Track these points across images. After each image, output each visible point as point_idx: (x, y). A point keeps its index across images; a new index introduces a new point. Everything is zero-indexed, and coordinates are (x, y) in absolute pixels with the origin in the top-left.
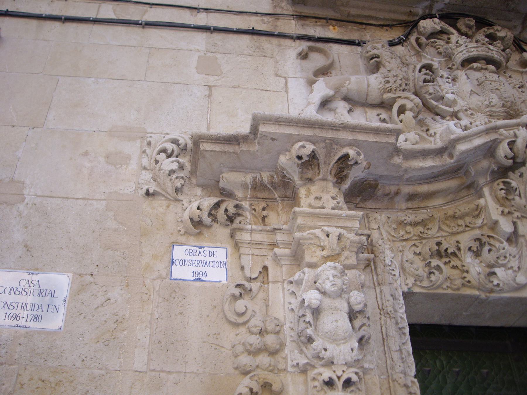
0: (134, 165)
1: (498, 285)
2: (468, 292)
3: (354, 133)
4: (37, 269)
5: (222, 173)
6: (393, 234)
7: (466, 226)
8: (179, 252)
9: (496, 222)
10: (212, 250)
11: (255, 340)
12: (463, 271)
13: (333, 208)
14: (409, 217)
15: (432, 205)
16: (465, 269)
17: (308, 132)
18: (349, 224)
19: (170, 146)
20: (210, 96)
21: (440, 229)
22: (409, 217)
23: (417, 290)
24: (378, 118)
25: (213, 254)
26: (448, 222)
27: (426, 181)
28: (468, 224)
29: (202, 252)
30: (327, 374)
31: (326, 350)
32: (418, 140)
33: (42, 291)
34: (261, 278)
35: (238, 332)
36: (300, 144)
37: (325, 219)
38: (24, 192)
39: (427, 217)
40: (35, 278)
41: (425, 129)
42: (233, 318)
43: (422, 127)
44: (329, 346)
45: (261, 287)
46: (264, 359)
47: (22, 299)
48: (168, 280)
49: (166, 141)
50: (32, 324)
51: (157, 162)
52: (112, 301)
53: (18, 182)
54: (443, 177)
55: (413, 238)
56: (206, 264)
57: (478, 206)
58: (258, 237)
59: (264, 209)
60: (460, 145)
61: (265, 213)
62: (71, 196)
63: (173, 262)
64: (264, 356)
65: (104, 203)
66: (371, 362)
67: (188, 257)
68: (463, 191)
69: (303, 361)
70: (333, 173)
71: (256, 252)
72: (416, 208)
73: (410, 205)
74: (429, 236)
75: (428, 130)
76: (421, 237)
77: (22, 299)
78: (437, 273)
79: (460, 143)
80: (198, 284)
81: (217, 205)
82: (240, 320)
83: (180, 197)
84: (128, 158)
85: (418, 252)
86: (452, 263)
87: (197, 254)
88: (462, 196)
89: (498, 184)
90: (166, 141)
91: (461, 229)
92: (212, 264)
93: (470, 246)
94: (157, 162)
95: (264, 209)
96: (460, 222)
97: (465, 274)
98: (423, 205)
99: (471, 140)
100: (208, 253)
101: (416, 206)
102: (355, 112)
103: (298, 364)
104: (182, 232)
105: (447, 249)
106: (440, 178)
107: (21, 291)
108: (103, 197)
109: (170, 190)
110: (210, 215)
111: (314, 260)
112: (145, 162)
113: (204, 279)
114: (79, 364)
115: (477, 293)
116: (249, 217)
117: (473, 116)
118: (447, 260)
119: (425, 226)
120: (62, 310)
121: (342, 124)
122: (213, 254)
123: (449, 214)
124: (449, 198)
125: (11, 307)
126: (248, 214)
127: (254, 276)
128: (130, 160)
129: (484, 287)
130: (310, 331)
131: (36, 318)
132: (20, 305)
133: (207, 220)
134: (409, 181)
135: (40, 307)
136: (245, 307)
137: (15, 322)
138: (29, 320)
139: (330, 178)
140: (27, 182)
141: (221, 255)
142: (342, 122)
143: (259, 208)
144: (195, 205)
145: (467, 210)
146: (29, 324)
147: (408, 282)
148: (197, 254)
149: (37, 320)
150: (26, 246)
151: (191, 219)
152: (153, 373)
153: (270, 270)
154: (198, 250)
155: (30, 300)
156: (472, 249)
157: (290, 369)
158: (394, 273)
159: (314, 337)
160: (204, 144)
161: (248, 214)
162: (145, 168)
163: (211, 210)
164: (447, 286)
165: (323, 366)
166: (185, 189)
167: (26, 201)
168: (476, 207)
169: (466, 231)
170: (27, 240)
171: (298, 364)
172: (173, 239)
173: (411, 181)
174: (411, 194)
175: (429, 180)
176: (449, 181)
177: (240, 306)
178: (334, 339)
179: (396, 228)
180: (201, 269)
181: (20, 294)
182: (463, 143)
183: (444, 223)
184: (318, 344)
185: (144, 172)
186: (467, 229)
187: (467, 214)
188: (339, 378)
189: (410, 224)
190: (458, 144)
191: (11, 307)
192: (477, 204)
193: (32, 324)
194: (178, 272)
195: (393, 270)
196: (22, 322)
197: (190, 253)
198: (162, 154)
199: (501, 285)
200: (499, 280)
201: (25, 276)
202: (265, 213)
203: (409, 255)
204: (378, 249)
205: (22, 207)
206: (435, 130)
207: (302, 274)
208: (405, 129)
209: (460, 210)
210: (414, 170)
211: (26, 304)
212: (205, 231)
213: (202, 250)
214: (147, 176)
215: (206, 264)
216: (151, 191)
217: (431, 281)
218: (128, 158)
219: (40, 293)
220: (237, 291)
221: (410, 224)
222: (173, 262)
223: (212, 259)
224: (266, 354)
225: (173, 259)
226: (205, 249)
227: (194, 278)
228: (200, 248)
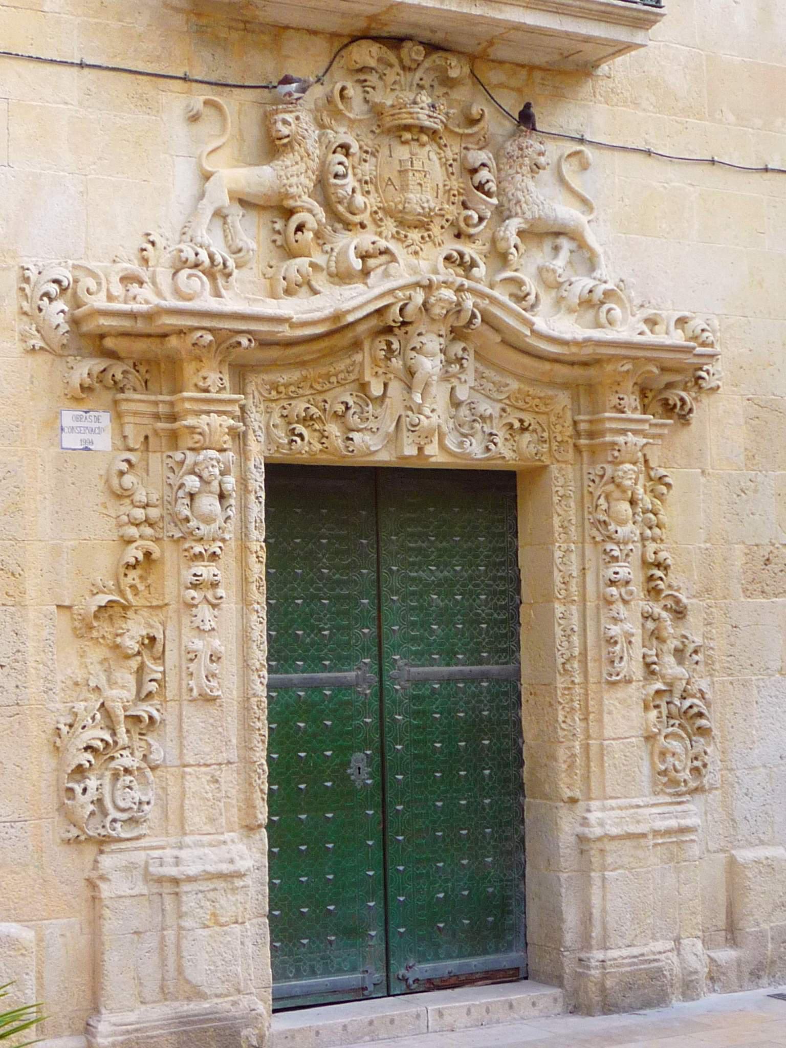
10: (97, 414)
25: (98, 419)
56: (92, 431)
63: (62, 429)
71: (138, 420)
113: (91, 447)
122: (98, 419)
141: (106, 418)
180: (87, 436)
197: (78, 418)
202: (147, 376)
213: (88, 415)
215: (92, 431)
223: (97, 425)
226: (91, 413)
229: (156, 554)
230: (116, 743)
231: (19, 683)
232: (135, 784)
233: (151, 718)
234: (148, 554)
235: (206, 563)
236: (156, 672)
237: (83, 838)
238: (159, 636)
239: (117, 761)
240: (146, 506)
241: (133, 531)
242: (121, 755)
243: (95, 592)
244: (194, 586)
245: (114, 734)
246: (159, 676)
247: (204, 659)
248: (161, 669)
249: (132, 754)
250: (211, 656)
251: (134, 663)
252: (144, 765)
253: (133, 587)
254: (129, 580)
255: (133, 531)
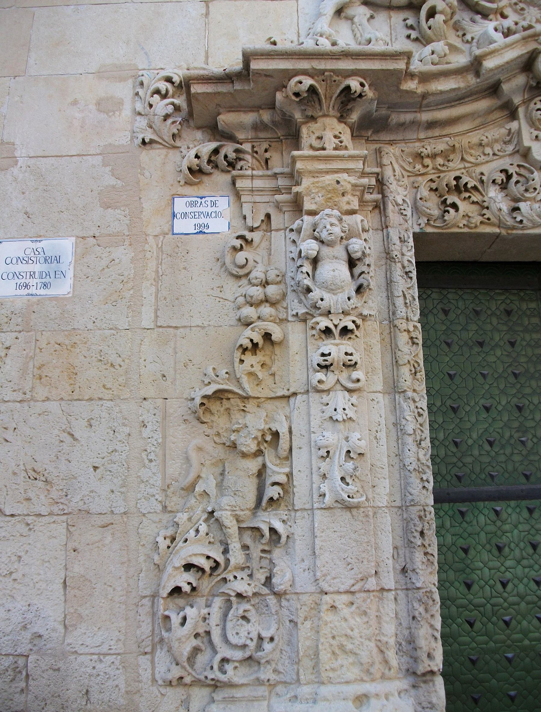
0: (127, 112)
1: (521, 221)
2: (488, 229)
3: (357, 61)
4: (40, 236)
5: (219, 114)
6: (408, 169)
7: (494, 154)
8: (180, 205)
9: (529, 149)
10: (213, 199)
11: (257, 292)
12: (483, 208)
13: (335, 149)
14: (426, 149)
15: (456, 132)
16: (486, 204)
17: (305, 65)
18: (351, 165)
19: (163, 86)
20: (207, 14)
21: (463, 159)
22: (426, 149)
23: (429, 230)
24: (402, 23)
25: (214, 204)
26: (473, 152)
27: (448, 105)
28: (497, 152)
29: (203, 203)
30: (324, 323)
31: (322, 300)
32: (447, 52)
33: (48, 258)
34: (264, 227)
35: (240, 284)
36: (297, 79)
37: (326, 161)
38: (16, 155)
39: (447, 147)
40: (39, 245)
41: (460, 33)
42: (235, 271)
43: (457, 31)
44: (326, 296)
45: (263, 237)
46: (266, 310)
47: (31, 268)
48: (170, 236)
49: (159, 80)
50: (43, 292)
51: (151, 106)
52: (117, 261)
53: (8, 143)
54: (470, 99)
55: (431, 172)
56: (208, 215)
57: (510, 130)
58: (258, 183)
59: (266, 151)
60: (487, 61)
61: (267, 155)
62: (64, 154)
63: (174, 215)
64: (265, 307)
65: (100, 158)
66: (370, 308)
67: (189, 210)
68: (495, 112)
69: (302, 311)
70: (336, 108)
72: (437, 137)
73: (430, 133)
74: (449, 169)
75: (464, 35)
76: (439, 170)
77: (31, 268)
78: (452, 211)
79: (487, 59)
80: (201, 236)
81: (216, 151)
82: (242, 272)
83: (178, 143)
84: (121, 103)
85: (434, 188)
86: (474, 198)
87: (198, 205)
88: (494, 118)
89: (535, 104)
90: (159, 80)
91: (486, 158)
92: (213, 215)
93: (494, 178)
94: (151, 106)
95: (266, 151)
96: (488, 150)
97: (485, 211)
98: (444, 133)
99: (502, 54)
100: (209, 203)
101: (437, 135)
102: (376, 19)
103: (297, 314)
104: (182, 183)
105: (466, 183)
106: (466, 100)
107: (27, 261)
108: (98, 151)
109: (168, 137)
110: (209, 162)
111: (313, 207)
112: (139, 106)
113: (206, 231)
114: (90, 326)
115: (497, 230)
116: (250, 161)
117: (522, 12)
118: (467, 195)
119: (446, 157)
120: (70, 274)
121: (342, 51)
122: (214, 204)
123: (473, 143)
124: (478, 121)
125: (20, 277)
126: (248, 157)
127: (256, 225)
128: (123, 104)
129: (506, 225)
130: (307, 282)
131: (45, 286)
132: (28, 274)
133: (208, 168)
134: (428, 107)
135: (48, 274)
136: (246, 259)
137: (25, 292)
138: (38, 288)
139: (332, 112)
140: (17, 142)
142: (343, 50)
143: (261, 150)
144: (193, 153)
145: (497, 136)
146: (39, 292)
147: (420, 221)
148: (198, 205)
149: (47, 287)
150: (26, 213)
151: (190, 169)
152: (161, 329)
153: (272, 218)
154: (199, 200)
155: (37, 268)
156: (497, 181)
157: (290, 319)
158: (405, 212)
159: (312, 287)
160: (196, 86)
161: (248, 157)
162: (140, 114)
163: (210, 157)
164: (464, 225)
165: (321, 315)
166: (184, 134)
167: (19, 164)
168: (507, 131)
169: (493, 160)
170: (25, 206)
171: (297, 314)
172: (174, 192)
173: (431, 106)
174: (429, 122)
175: (453, 104)
176: (477, 103)
177: (241, 257)
178: (332, 288)
179: (412, 161)
180: (202, 220)
181: (27, 263)
182: (492, 58)
183: (467, 153)
184: (316, 294)
185: (138, 118)
186: (495, 157)
187: (496, 141)
188: (336, 326)
189: (428, 156)
190: (485, 60)
191: (20, 277)
192: (508, 128)
193: (43, 292)
194: (181, 226)
195: (405, 210)
196: (33, 290)
197: (192, 204)
198: (155, 96)
199: (524, 222)
200: (523, 216)
201: (29, 244)
202: (267, 155)
203: (424, 192)
204: (388, 188)
205: (15, 170)
206: (473, 35)
207: (301, 222)
208: (434, 38)
209: (487, 137)
210: (433, 94)
211: (34, 273)
212: (205, 179)
213: (203, 200)
214: (142, 122)
215: (208, 215)
216: (147, 140)
217: (445, 221)
218: (121, 103)
219: (46, 260)
220: (238, 243)
221: (428, 156)
222: (174, 216)
223: (214, 209)
224: (268, 305)
225: (174, 213)
226: (207, 199)
227: (196, 231)
228: (201, 198)
229: (277, 335)
230: (228, 561)
231: (114, 489)
232: (252, 615)
233: (272, 530)
234: (267, 336)
235: (337, 341)
236: (279, 473)
237: (188, 680)
238: (283, 431)
239: (229, 585)
240: (266, 283)
241: (249, 312)
242: (235, 577)
243: (206, 382)
244: (325, 367)
245: (226, 551)
246: (282, 479)
247: (339, 457)
248: (287, 470)
249: (251, 576)
250: (349, 452)
251: (254, 465)
252: (265, 590)
253: (251, 374)
254: (246, 366)
255: (249, 312)
